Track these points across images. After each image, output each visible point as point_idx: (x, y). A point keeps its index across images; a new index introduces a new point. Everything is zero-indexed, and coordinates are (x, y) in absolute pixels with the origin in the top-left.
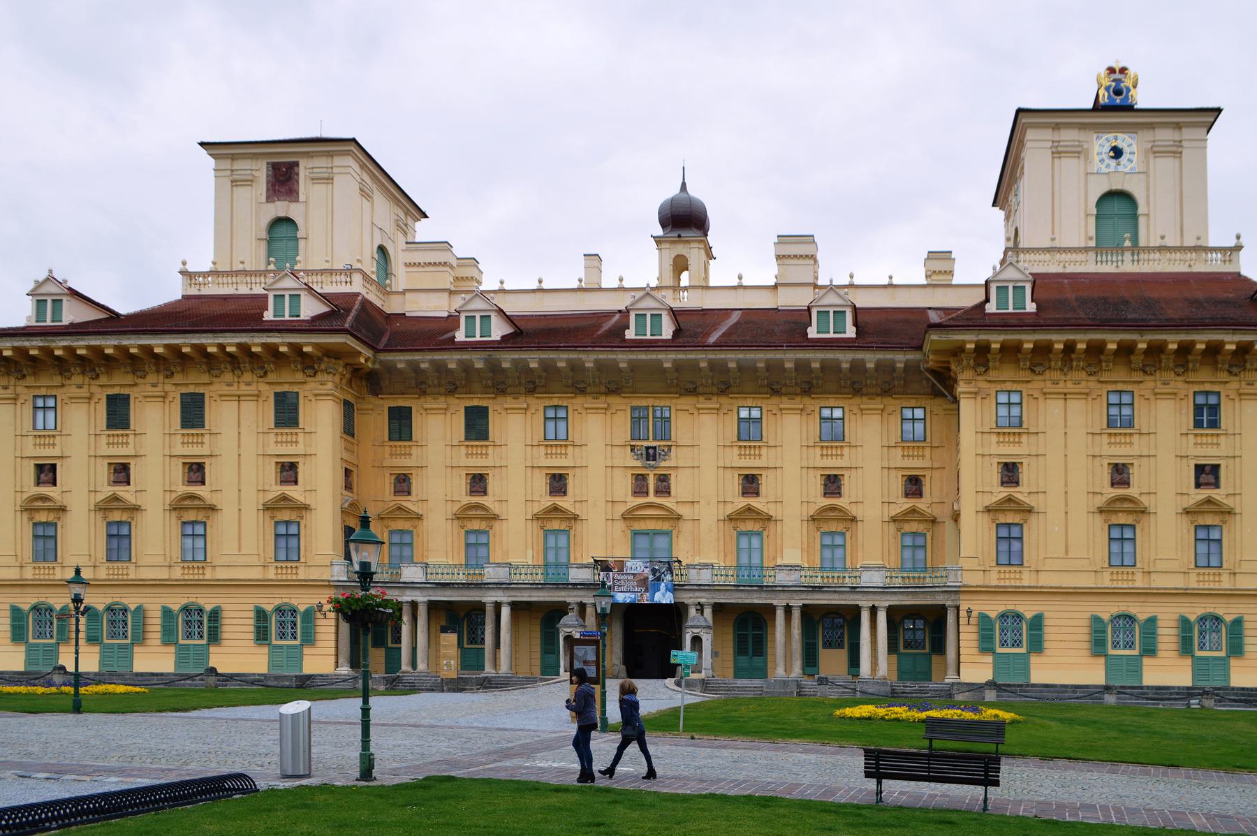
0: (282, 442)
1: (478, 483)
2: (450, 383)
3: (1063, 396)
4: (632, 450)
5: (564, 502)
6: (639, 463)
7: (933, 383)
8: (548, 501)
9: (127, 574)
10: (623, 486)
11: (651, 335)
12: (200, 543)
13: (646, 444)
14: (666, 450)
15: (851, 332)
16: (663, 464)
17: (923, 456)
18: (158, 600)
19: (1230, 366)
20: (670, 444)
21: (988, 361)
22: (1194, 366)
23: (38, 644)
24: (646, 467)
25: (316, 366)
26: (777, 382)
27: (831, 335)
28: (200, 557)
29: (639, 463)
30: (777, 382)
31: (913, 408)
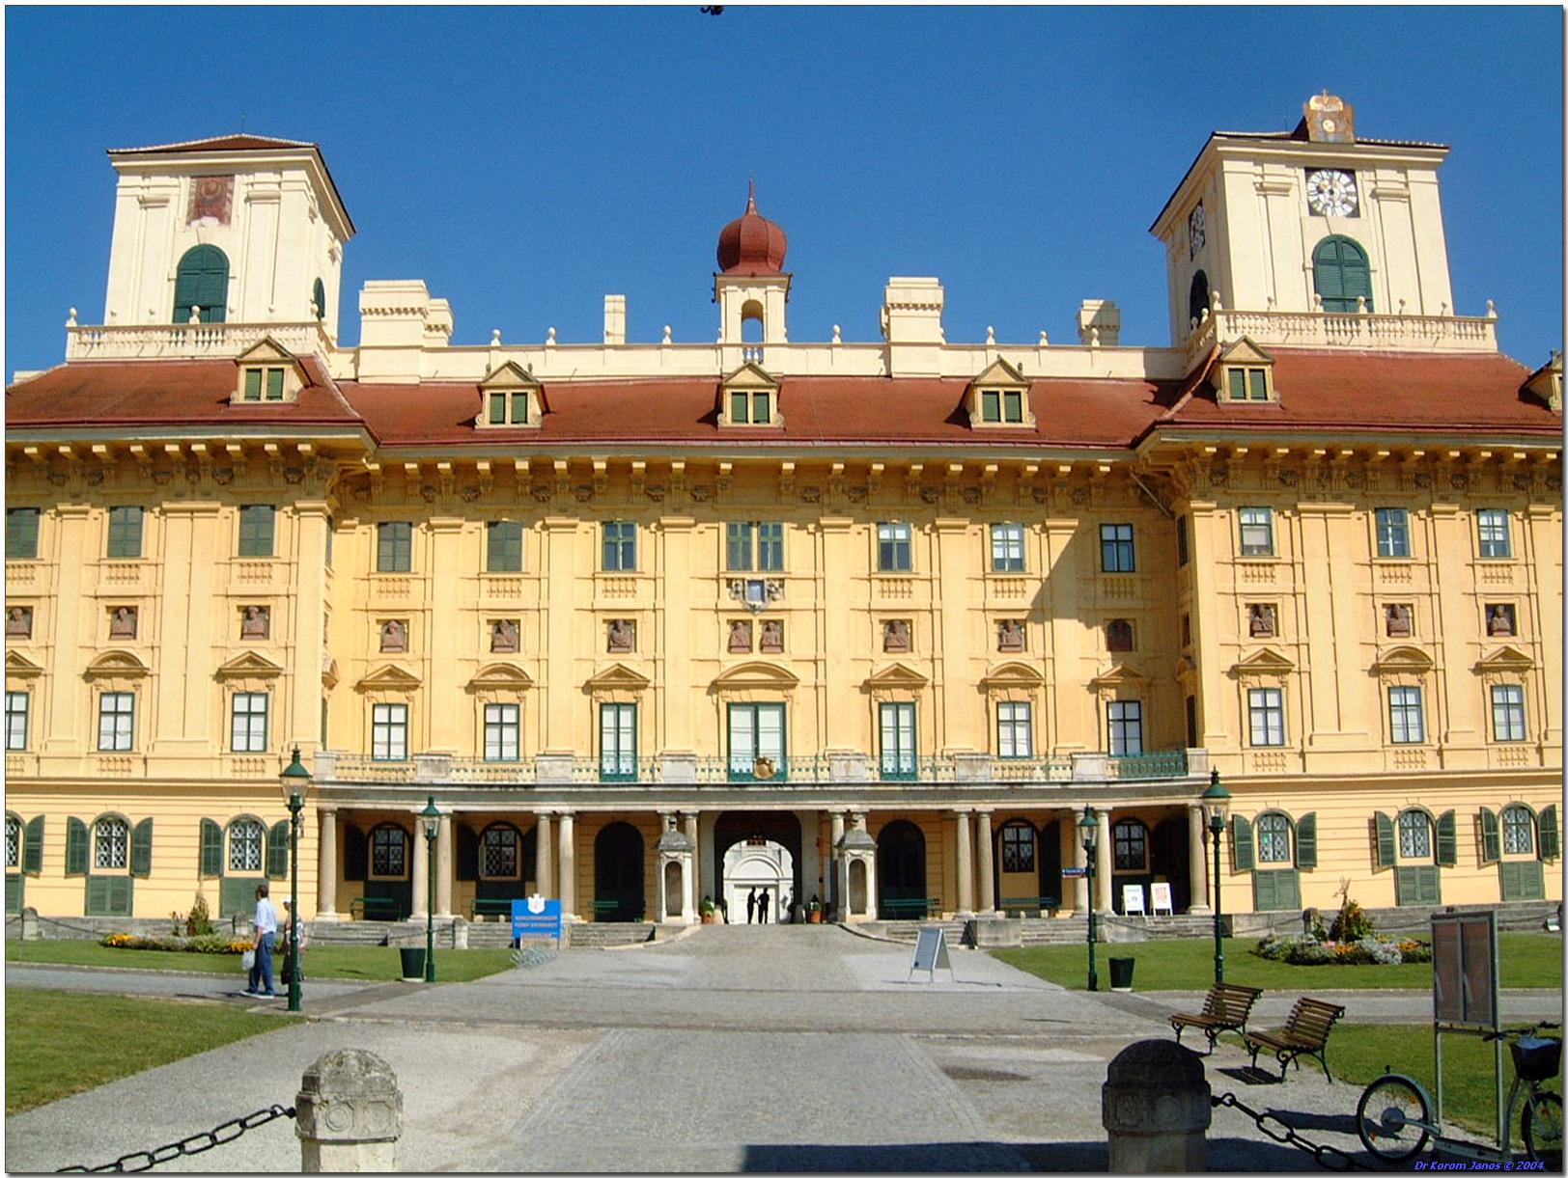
1: (504, 631)
2: (468, 488)
3: (1322, 515)
4: (729, 585)
5: (632, 662)
6: (738, 605)
7: (1143, 492)
8: (607, 662)
9: (22, 770)
10: (713, 635)
11: (755, 422)
13: (748, 576)
14: (777, 584)
15: (1028, 422)
16: (772, 605)
17: (1132, 593)
18: (63, 808)
19: (1516, 477)
20: (782, 576)
21: (1227, 467)
22: (1476, 477)
24: (746, 611)
25: (305, 471)
26: (931, 489)
27: (1004, 424)
30: (931, 489)
31: (1116, 526)
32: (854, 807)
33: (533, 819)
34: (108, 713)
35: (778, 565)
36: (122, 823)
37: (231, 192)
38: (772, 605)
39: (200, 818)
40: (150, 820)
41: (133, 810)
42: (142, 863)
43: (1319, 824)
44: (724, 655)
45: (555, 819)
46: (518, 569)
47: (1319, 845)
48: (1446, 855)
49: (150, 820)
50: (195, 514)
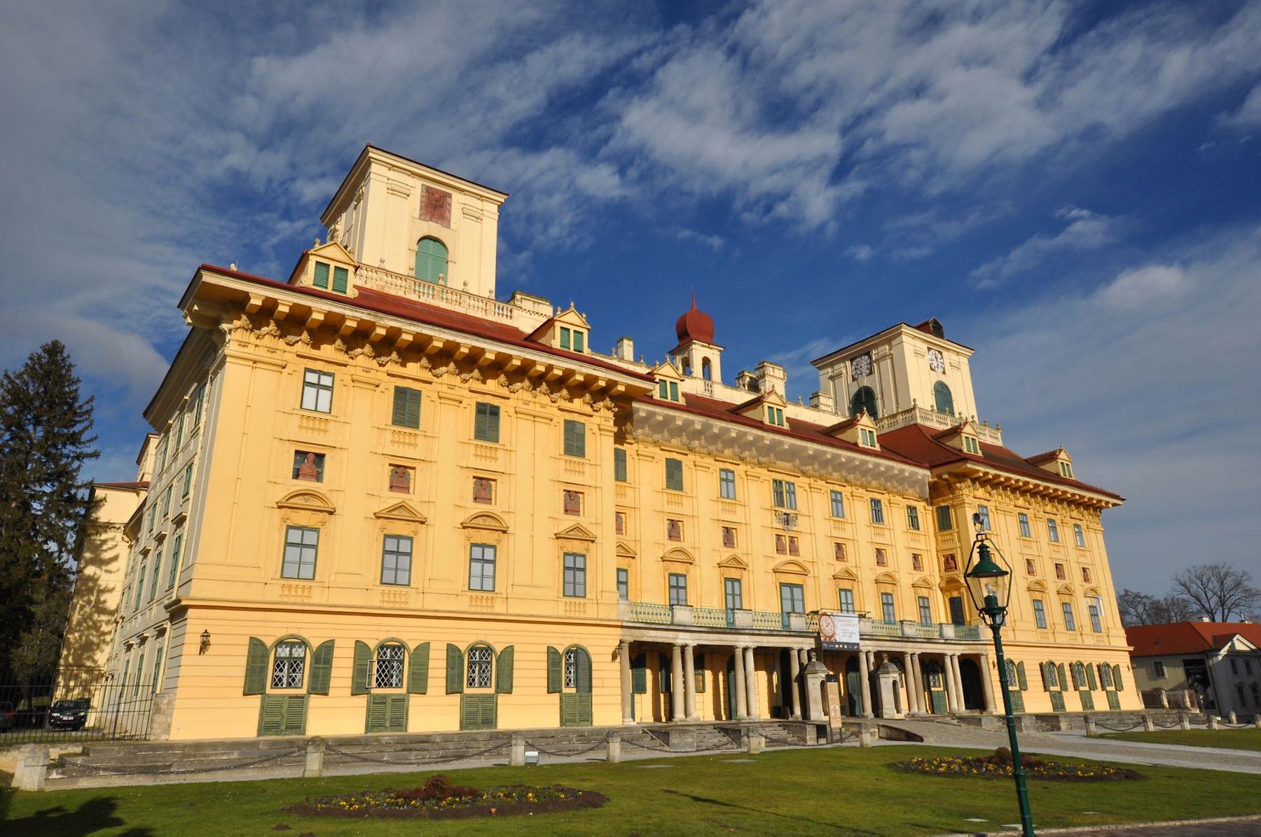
0: (570, 470)
12: (488, 568)
16: (794, 528)
23: (384, 697)
27: (869, 447)
28: (488, 585)
29: (780, 526)
32: (870, 648)
33: (731, 649)
34: (477, 560)
35: (793, 506)
36: (488, 650)
37: (450, 205)
38: (794, 528)
39: (546, 646)
40: (512, 647)
41: (497, 637)
42: (505, 686)
43: (1026, 667)
44: (776, 555)
45: (745, 650)
46: (681, 489)
47: (1027, 678)
48: (1064, 687)
49: (512, 647)
50: (537, 419)
